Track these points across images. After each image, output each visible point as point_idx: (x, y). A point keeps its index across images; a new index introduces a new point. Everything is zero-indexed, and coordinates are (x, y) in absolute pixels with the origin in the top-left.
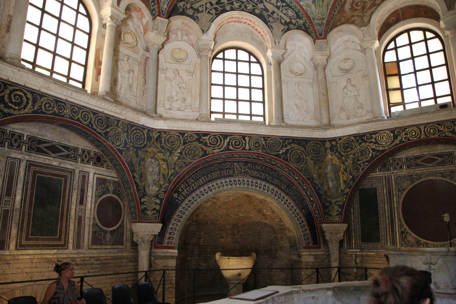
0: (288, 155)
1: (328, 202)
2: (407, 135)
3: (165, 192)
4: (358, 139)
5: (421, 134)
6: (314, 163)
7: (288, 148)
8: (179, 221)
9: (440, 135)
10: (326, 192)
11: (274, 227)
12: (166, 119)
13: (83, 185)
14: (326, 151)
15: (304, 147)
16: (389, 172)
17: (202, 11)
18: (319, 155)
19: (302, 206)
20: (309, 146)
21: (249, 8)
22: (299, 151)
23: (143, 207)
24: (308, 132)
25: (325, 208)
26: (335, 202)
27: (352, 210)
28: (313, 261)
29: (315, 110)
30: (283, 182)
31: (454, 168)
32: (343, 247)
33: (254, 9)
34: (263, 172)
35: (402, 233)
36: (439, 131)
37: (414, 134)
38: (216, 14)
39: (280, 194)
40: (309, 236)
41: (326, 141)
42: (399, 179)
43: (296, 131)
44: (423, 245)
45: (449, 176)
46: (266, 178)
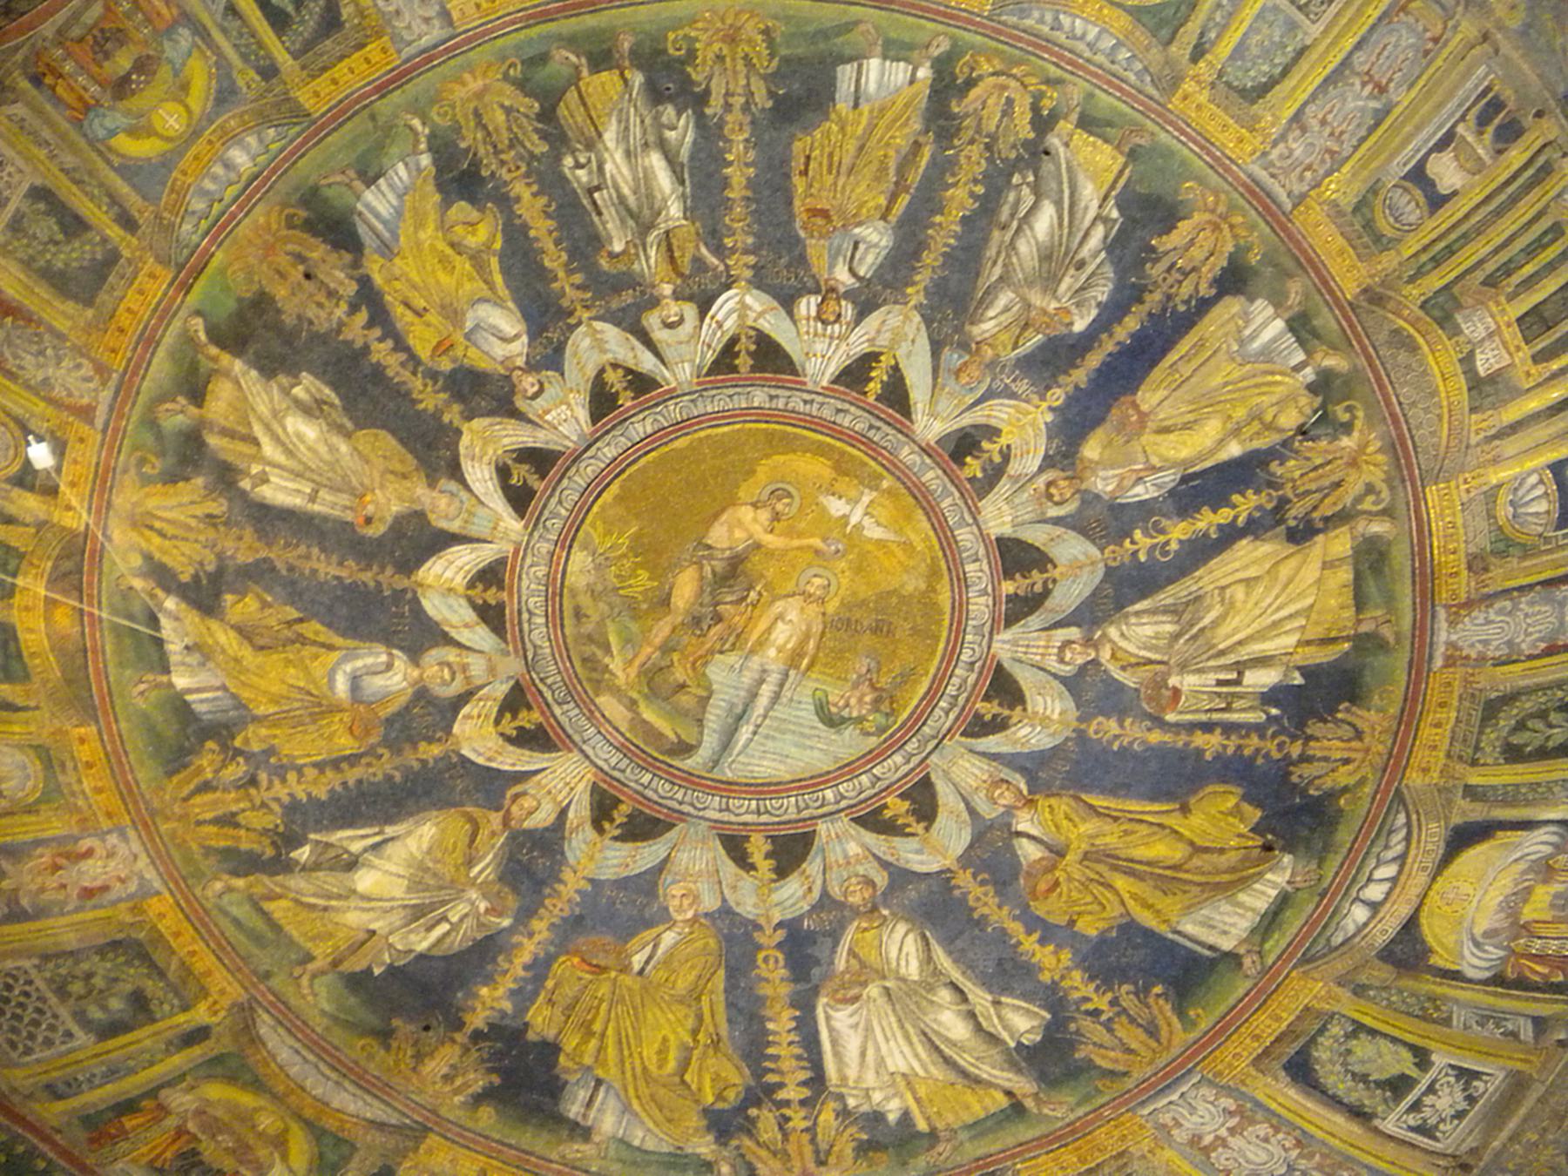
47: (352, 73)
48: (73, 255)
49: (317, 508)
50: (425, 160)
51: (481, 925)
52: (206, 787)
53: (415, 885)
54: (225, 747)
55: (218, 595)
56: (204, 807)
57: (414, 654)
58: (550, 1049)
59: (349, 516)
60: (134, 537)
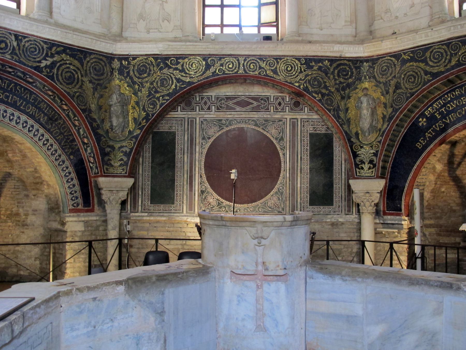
0: (55, 71)
1: (109, 146)
2: (223, 66)
4: (160, 62)
5: (239, 68)
6: (93, 88)
7: (55, 59)
9: (260, 72)
10: (107, 132)
11: (25, 180)
14: (112, 73)
16: (195, 113)
18: (102, 77)
19: (71, 150)
20: (88, 62)
22: (72, 67)
24: (90, 40)
25: (105, 155)
26: (120, 148)
27: (141, 159)
28: (83, 229)
29: (102, 10)
30: (43, 112)
31: (269, 116)
32: (125, 210)
35: (202, 192)
36: (260, 68)
37: (230, 66)
39: (38, 131)
40: (79, 194)
41: (114, 58)
42: (205, 123)
43: (70, 35)
44: (225, 207)
45: (262, 125)
46: (15, 102)
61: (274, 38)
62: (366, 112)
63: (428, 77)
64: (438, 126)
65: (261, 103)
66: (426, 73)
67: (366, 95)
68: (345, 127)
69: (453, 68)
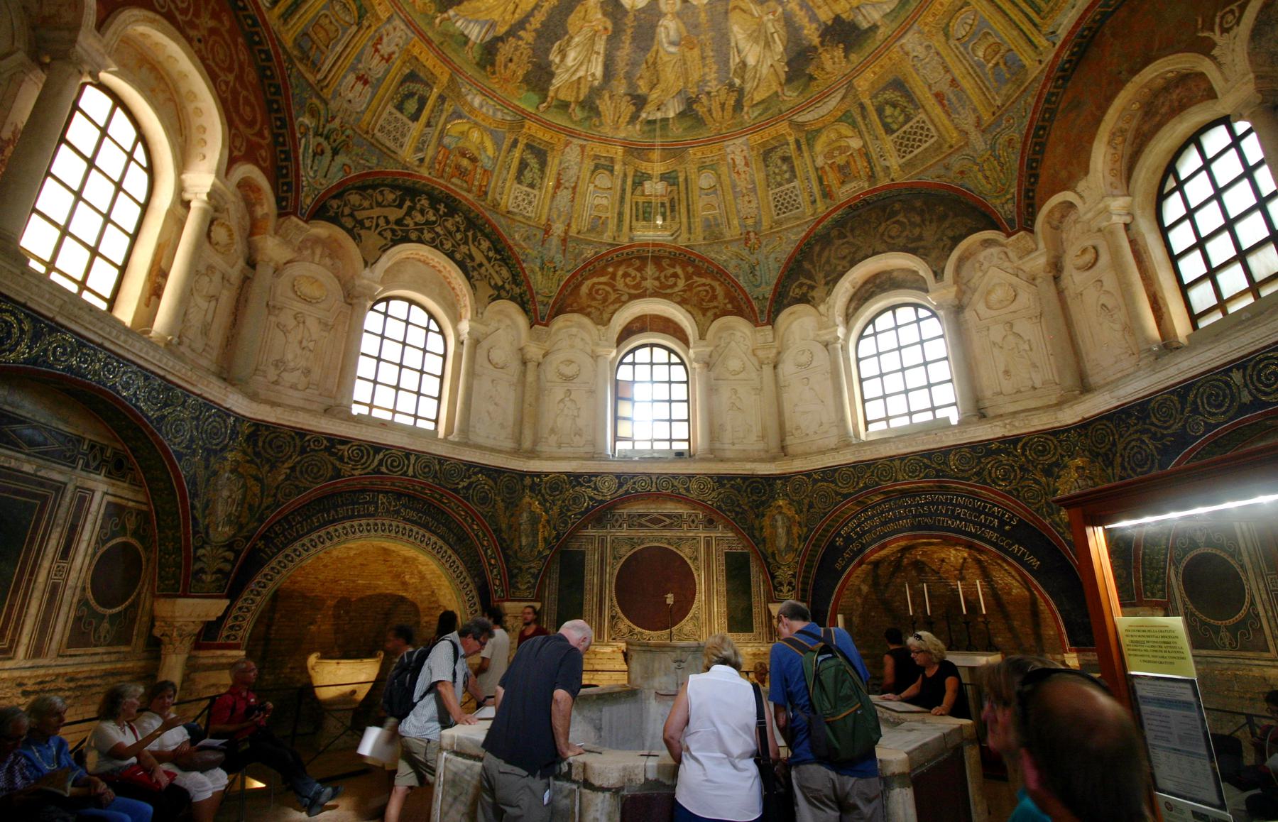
3: (248, 539)
8: (259, 594)
12: (274, 404)
13: (77, 517)
15: (494, 480)
17: (369, 228)
21: (447, 247)
23: (198, 566)
25: (511, 578)
33: (453, 252)
34: (424, 513)
35: (613, 617)
38: (392, 240)
47: (429, 60)
48: (533, 162)
49: (602, 51)
50: (451, 13)
51: (778, 20)
52: (710, 111)
53: (756, 41)
54: (695, 102)
55: (639, 96)
56: (717, 114)
57: (661, 15)
58: (837, 19)
59: (604, 37)
60: (622, 127)
61: (687, 455)
62: (781, 531)
63: (839, 498)
64: (855, 546)
65: (674, 521)
66: (837, 494)
67: (780, 513)
68: (761, 546)
69: (861, 490)
